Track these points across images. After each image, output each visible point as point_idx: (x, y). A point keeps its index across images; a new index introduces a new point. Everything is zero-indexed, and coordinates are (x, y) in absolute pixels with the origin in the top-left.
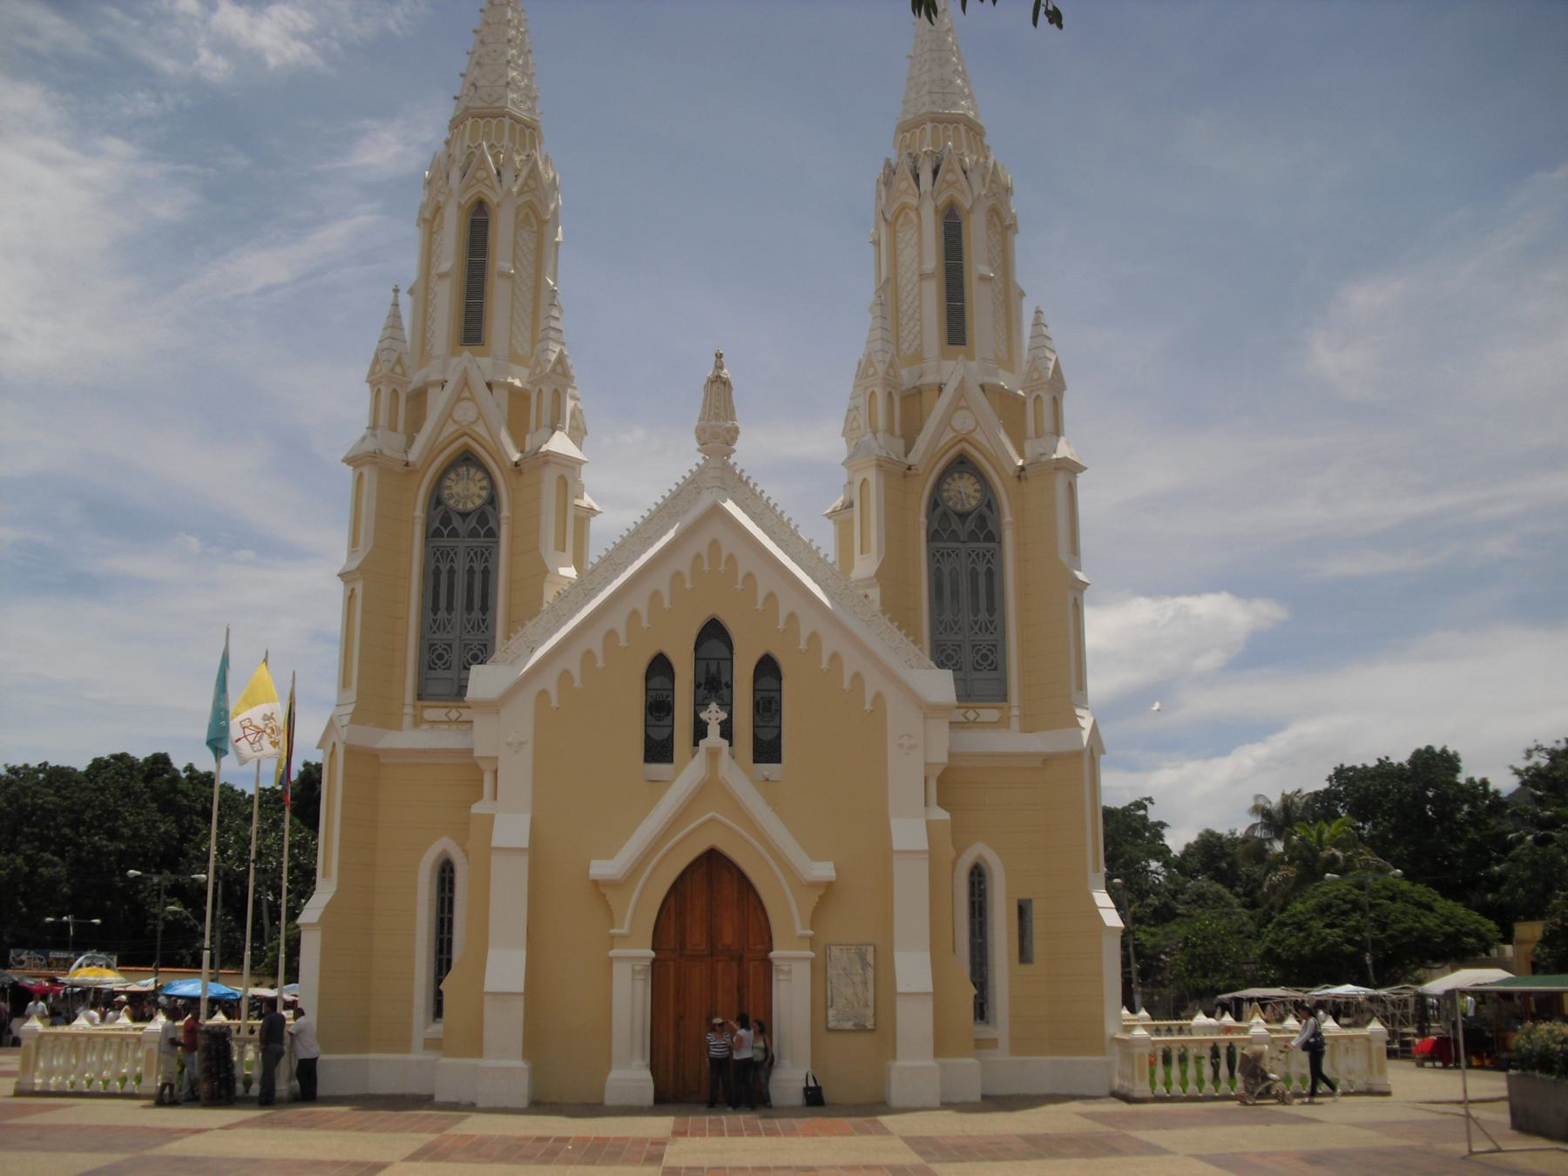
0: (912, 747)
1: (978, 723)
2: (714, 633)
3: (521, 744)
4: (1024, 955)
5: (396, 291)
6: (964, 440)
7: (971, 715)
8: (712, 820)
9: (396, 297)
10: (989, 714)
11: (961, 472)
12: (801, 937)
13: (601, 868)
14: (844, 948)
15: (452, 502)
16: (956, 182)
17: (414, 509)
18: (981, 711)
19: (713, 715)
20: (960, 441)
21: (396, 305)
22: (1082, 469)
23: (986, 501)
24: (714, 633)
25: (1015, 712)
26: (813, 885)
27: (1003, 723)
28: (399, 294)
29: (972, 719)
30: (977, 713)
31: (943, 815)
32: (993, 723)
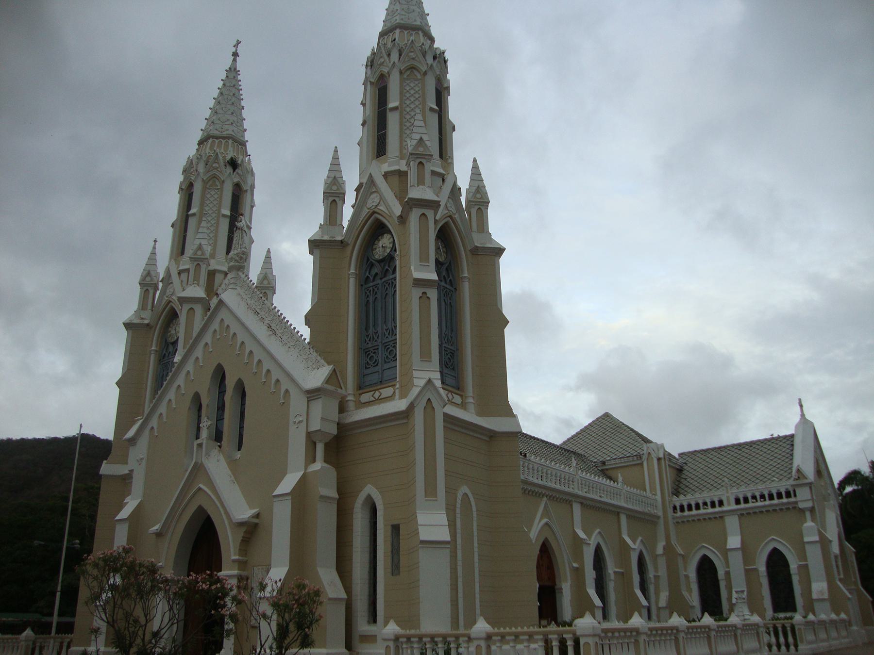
0: (300, 422)
1: (382, 399)
2: (220, 375)
3: (142, 459)
4: (395, 568)
5: (155, 241)
6: (374, 212)
7: (377, 394)
8: (200, 489)
9: (155, 244)
10: (387, 392)
11: (382, 234)
12: (234, 561)
13: (157, 527)
14: (260, 567)
15: (170, 339)
16: (383, 62)
17: (151, 346)
18: (380, 390)
19: (205, 424)
20: (373, 214)
21: (154, 248)
22: (440, 201)
23: (394, 249)
24: (220, 375)
25: (397, 386)
26: (241, 524)
27: (391, 398)
28: (157, 243)
29: (377, 398)
30: (380, 392)
31: (318, 466)
32: (389, 397)
